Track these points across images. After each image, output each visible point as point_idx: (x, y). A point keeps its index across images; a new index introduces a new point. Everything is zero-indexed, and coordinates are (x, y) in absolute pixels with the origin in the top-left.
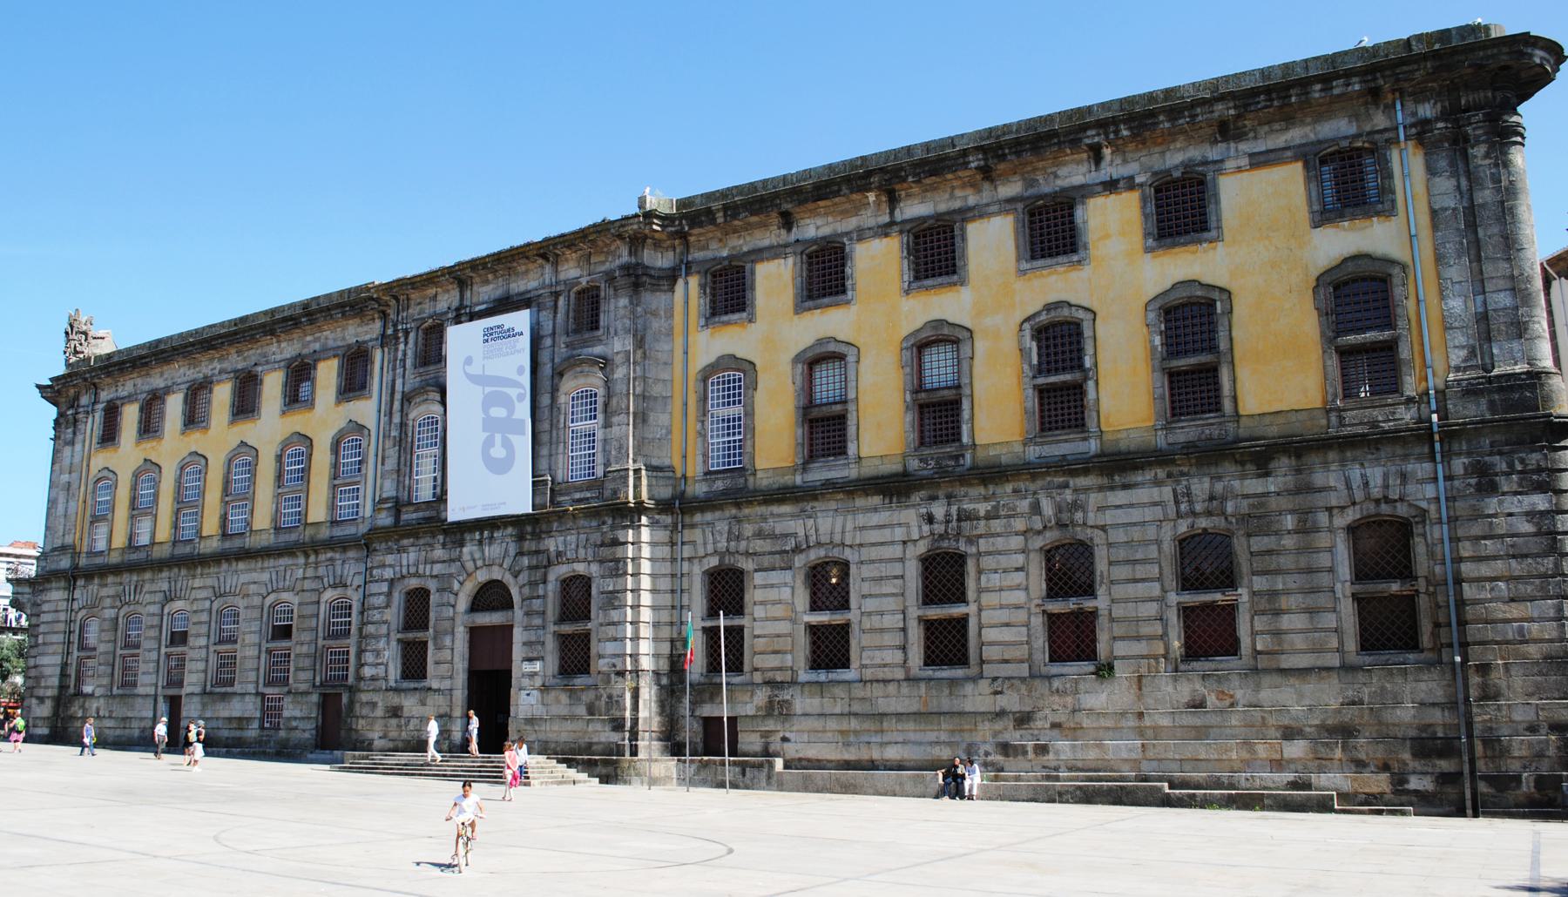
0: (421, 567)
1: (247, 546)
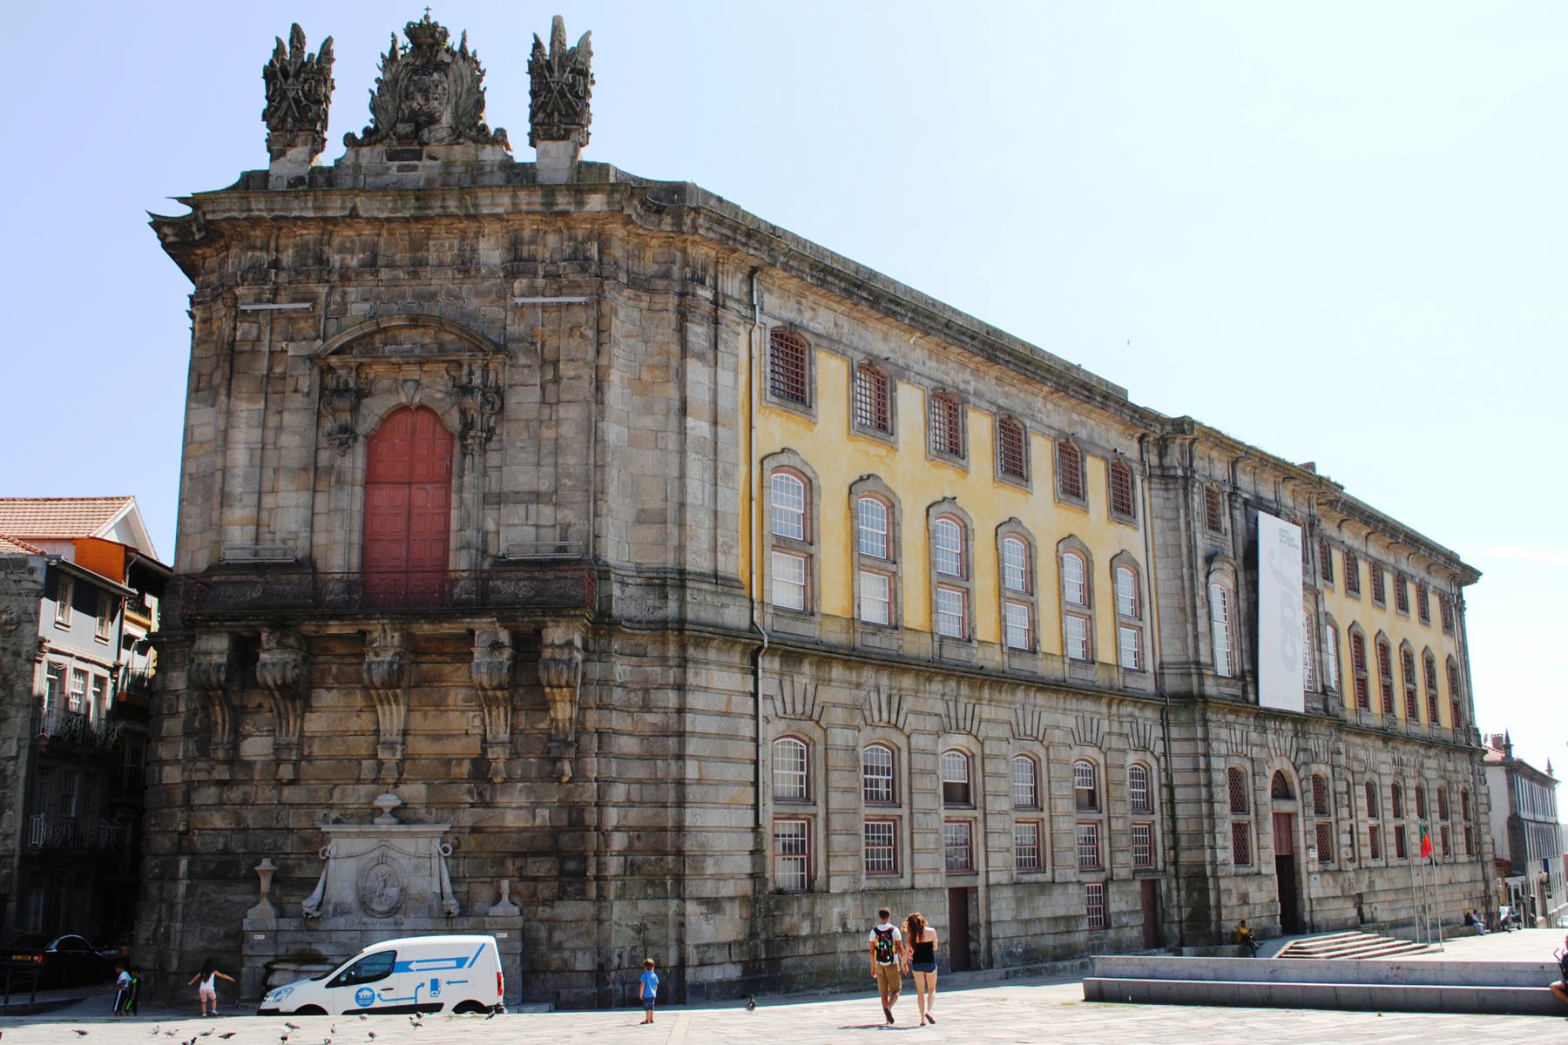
1: (975, 661)
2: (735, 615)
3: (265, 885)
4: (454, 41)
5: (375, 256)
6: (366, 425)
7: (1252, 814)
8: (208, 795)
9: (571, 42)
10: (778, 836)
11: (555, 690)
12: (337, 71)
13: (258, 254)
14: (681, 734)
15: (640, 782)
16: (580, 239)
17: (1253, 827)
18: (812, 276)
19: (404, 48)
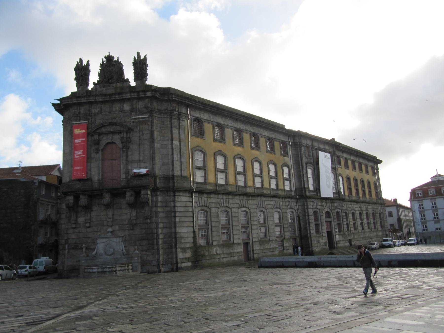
0: (317, 206)
2: (186, 185)
3: (84, 250)
4: (116, 59)
5: (101, 109)
6: (101, 147)
7: (320, 222)
8: (71, 231)
9: (142, 57)
10: (200, 233)
11: (145, 204)
12: (90, 68)
13: (75, 111)
14: (175, 212)
15: (165, 223)
16: (146, 102)
17: (320, 225)
18: (202, 106)
19: (105, 61)
